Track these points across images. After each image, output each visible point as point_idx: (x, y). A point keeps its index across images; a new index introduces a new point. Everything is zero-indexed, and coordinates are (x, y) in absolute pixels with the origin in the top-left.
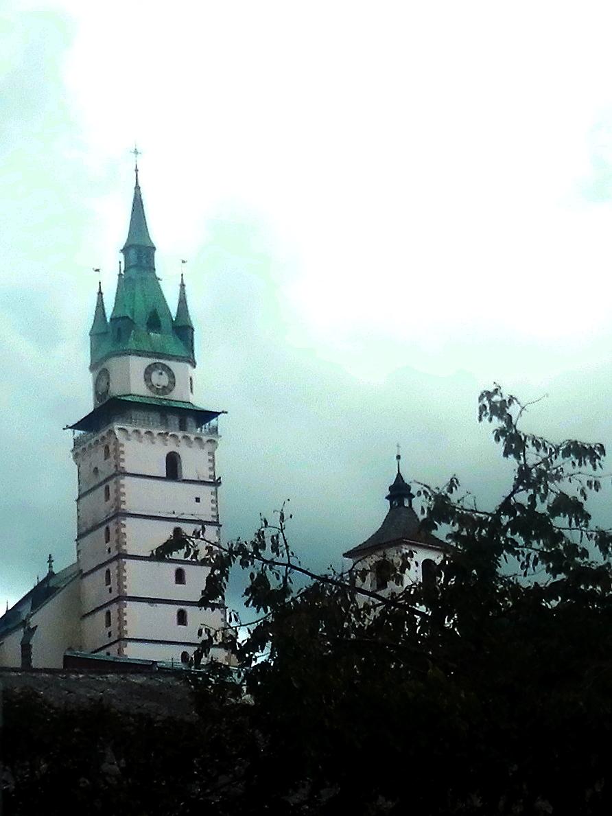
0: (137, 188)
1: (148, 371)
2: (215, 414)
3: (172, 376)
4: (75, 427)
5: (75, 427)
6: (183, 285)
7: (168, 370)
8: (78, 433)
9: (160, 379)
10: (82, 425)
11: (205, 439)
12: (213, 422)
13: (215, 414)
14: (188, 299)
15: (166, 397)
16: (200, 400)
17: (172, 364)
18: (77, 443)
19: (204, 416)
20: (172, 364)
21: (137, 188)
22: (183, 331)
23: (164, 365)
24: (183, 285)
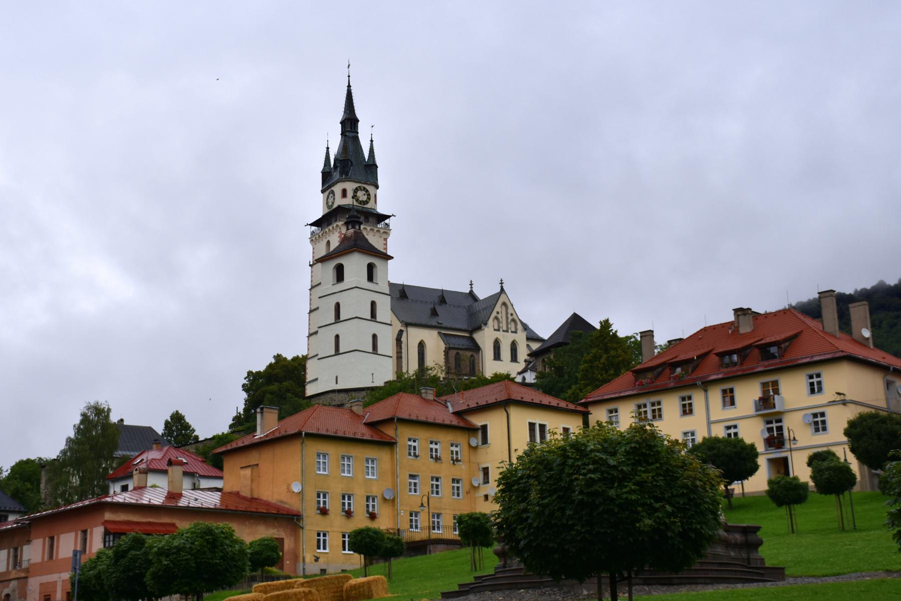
0: (349, 86)
1: (356, 191)
2: (388, 217)
4: (312, 225)
5: (312, 225)
6: (372, 141)
7: (367, 191)
8: (314, 228)
9: (361, 195)
10: (316, 224)
11: (382, 231)
12: (387, 221)
13: (388, 217)
16: (381, 209)
17: (367, 187)
18: (313, 233)
21: (349, 86)
22: (371, 168)
24: (372, 141)
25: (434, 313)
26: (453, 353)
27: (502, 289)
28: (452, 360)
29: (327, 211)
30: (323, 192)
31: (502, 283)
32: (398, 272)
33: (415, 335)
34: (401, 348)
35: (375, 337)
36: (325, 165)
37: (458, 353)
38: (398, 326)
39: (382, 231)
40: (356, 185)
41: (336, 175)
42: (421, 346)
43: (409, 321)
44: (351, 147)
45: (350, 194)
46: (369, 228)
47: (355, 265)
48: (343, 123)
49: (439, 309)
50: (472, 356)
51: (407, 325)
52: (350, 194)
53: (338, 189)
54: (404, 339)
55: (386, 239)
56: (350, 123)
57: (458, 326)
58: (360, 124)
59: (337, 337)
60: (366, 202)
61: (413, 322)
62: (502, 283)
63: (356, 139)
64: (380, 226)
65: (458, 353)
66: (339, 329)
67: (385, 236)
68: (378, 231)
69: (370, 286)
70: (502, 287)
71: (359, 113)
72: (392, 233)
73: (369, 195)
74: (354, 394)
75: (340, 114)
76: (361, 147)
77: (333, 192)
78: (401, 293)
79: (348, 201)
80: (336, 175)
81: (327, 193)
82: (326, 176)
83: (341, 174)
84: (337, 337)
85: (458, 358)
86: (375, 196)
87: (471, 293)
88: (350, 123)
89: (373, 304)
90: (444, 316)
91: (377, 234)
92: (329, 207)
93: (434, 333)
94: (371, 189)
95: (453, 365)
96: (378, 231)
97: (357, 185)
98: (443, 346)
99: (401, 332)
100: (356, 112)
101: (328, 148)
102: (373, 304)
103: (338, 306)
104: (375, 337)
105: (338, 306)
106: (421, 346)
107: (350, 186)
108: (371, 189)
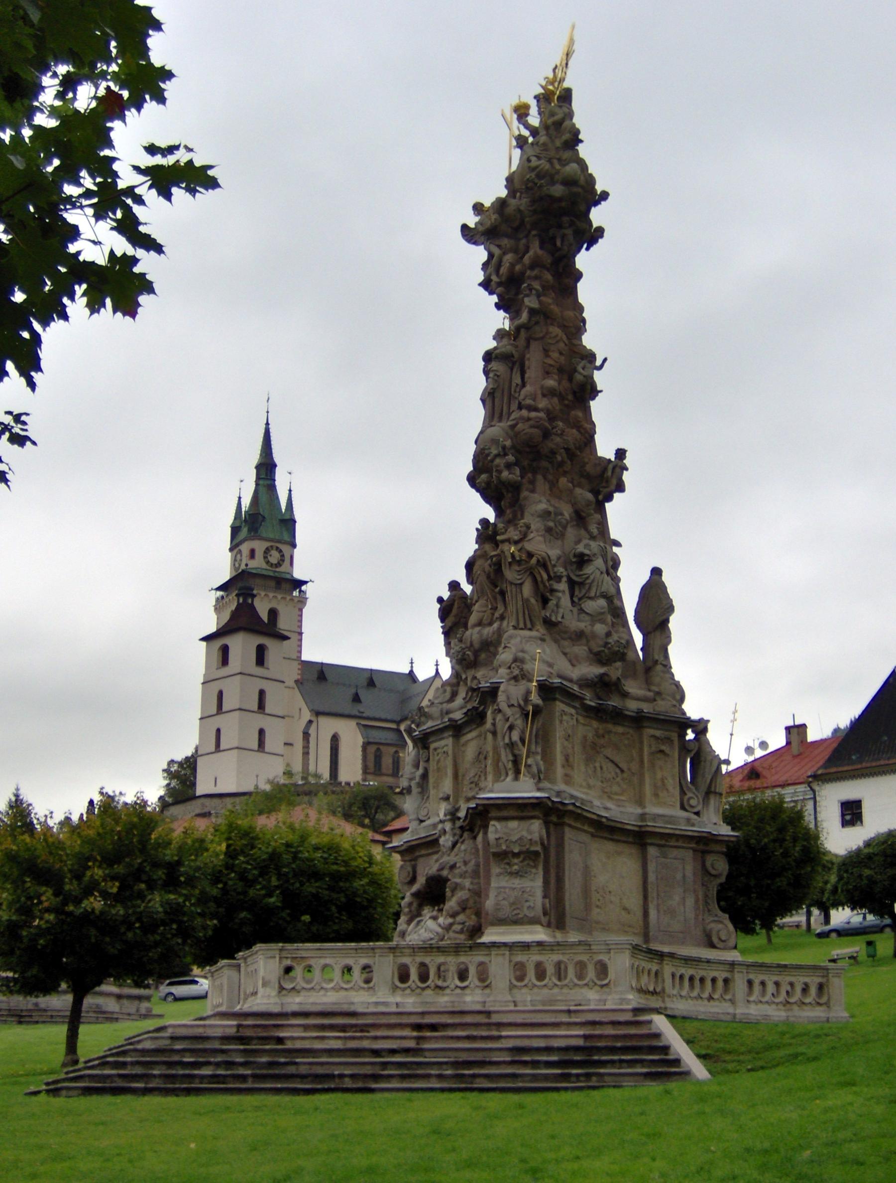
0: (267, 424)
1: (267, 551)
2: (305, 583)
6: (290, 491)
7: (280, 551)
9: (274, 557)
12: (304, 588)
13: (305, 583)
15: (277, 570)
17: (281, 546)
19: (299, 584)
20: (281, 546)
21: (267, 424)
22: (289, 523)
23: (277, 548)
24: (290, 491)
25: (356, 699)
26: (372, 749)
27: (437, 670)
28: (371, 757)
29: (234, 574)
30: (231, 550)
31: (437, 665)
32: (316, 649)
33: (328, 727)
34: (308, 742)
35: (261, 732)
36: (235, 519)
37: (378, 749)
38: (307, 715)
39: (296, 600)
40: (268, 544)
41: (244, 532)
42: (335, 739)
43: (321, 709)
44: (264, 498)
45: (259, 554)
46: (279, 597)
47: (241, 646)
48: (258, 467)
49: (363, 694)
50: (396, 752)
51: (318, 714)
52: (259, 554)
53: (245, 548)
54: (312, 731)
55: (301, 610)
56: (266, 468)
57: (383, 717)
58: (278, 471)
59: (218, 731)
60: (279, 565)
61: (327, 710)
62: (437, 665)
63: (272, 488)
64: (296, 593)
65: (378, 749)
66: (220, 721)
67: (299, 606)
68: (292, 600)
69: (259, 671)
70: (437, 670)
72: (309, 602)
73: (283, 556)
74: (228, 801)
75: (255, 457)
76: (278, 498)
77: (240, 551)
78: (321, 674)
79: (258, 564)
80: (244, 532)
81: (235, 551)
82: (235, 530)
83: (249, 531)
84: (218, 731)
85: (378, 757)
86: (292, 557)
87: (411, 672)
88: (266, 468)
89: (262, 693)
90: (371, 703)
92: (236, 569)
93: (352, 724)
94: (285, 548)
95: (371, 764)
96: (292, 600)
97: (268, 544)
98: (360, 741)
99: (310, 722)
100: (274, 456)
101: (240, 498)
102: (262, 693)
103: (220, 694)
104: (261, 732)
105: (220, 694)
106: (335, 739)
107: (260, 546)
108: (285, 548)
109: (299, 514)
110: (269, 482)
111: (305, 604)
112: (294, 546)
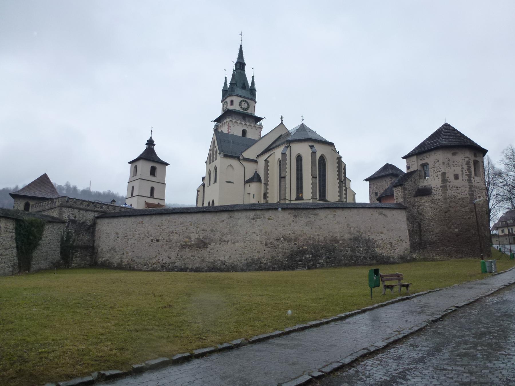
0: (241, 45)
2: (261, 119)
3: (248, 105)
7: (247, 103)
9: (244, 105)
13: (261, 119)
14: (255, 82)
16: (257, 114)
17: (248, 101)
20: (248, 101)
21: (241, 45)
22: (253, 91)
39: (257, 126)
40: (241, 99)
53: (229, 100)
56: (240, 65)
58: (246, 67)
60: (247, 109)
67: (259, 130)
71: (246, 60)
77: (226, 102)
79: (236, 107)
88: (240, 65)
91: (254, 128)
100: (244, 60)
109: (257, 87)
110: (242, 72)
111: (262, 128)
112: (256, 102)
